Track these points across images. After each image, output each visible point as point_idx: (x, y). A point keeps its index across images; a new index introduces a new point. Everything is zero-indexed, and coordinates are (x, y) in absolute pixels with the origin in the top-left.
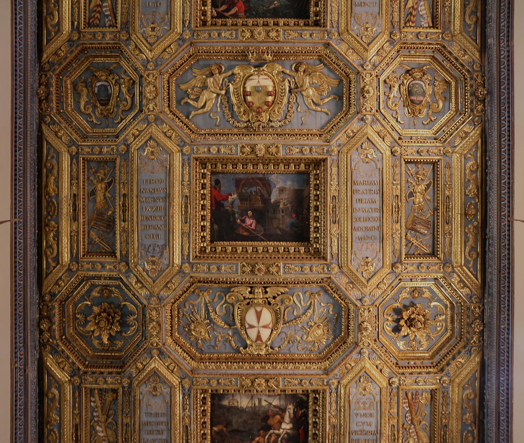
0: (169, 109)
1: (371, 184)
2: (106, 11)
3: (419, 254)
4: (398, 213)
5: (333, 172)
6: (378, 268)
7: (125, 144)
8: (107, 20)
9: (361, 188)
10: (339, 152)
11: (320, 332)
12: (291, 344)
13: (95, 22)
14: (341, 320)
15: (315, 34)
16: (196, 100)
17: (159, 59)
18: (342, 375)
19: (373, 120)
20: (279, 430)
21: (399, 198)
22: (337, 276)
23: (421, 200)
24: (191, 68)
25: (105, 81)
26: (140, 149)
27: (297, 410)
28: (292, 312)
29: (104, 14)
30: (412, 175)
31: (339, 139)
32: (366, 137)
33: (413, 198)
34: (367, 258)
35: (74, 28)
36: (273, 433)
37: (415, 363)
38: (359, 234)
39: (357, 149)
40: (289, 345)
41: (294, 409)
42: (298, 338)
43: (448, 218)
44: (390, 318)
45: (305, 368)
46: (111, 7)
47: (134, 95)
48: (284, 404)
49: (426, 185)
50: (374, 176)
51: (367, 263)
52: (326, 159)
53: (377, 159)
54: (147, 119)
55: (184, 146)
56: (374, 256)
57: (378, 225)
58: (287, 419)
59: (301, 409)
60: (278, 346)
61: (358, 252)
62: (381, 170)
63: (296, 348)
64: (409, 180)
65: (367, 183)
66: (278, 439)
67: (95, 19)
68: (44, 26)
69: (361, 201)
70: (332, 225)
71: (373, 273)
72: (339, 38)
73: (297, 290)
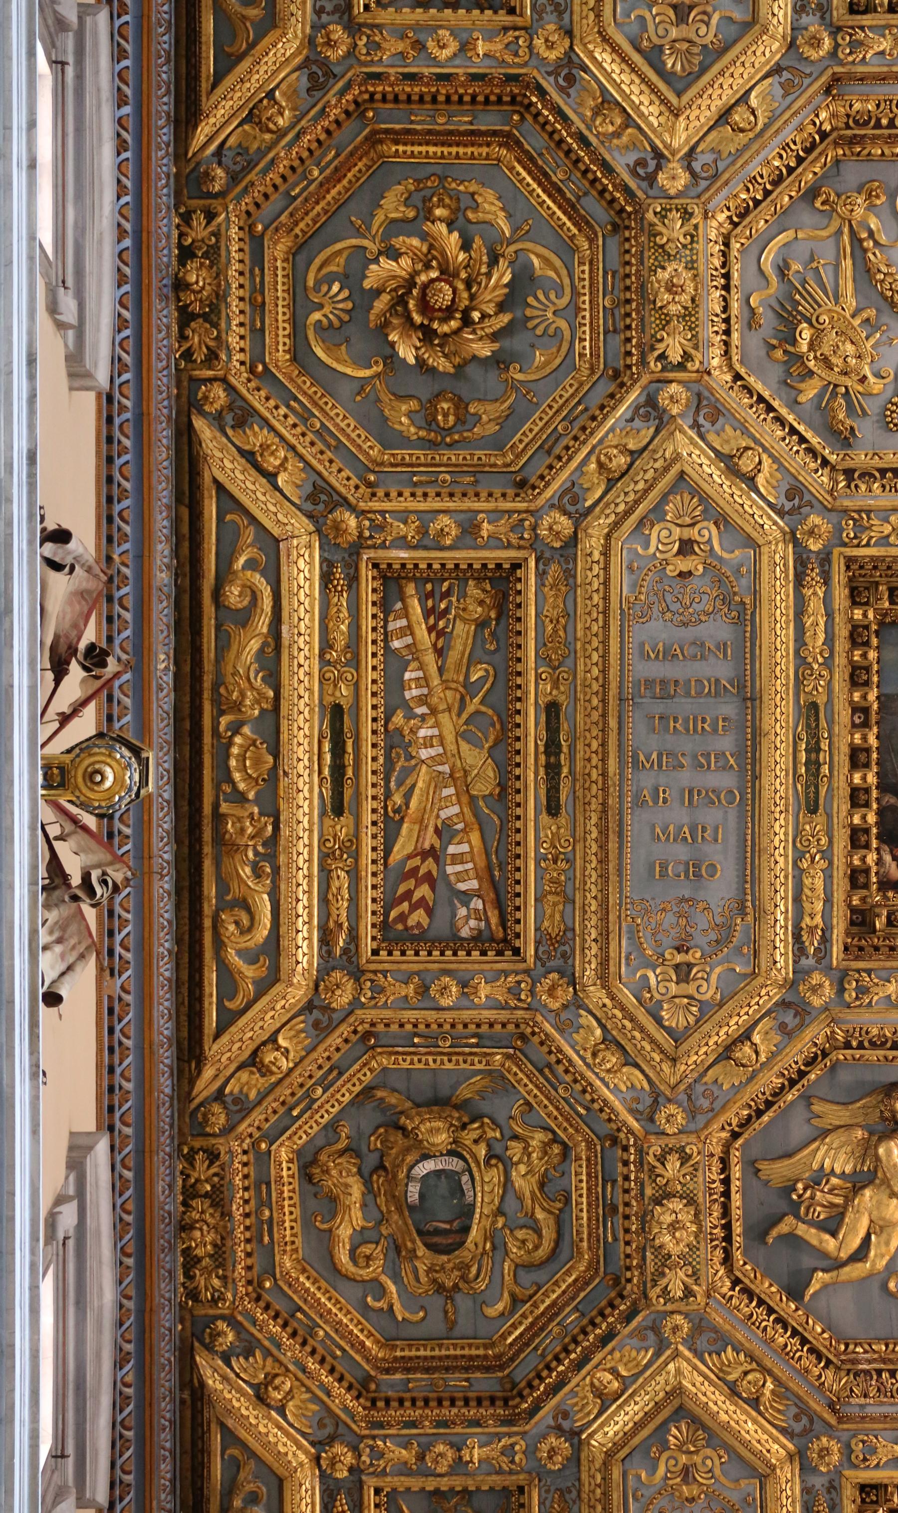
0: (730, 1271)
2: (461, 877)
7: (559, 1430)
8: (462, 912)
13: (411, 922)
16: (832, 1226)
17: (700, 1088)
24: (807, 1099)
25: (451, 1153)
26: (637, 1457)
29: (449, 884)
35: (329, 953)
46: (481, 863)
47: (567, 1200)
54: (656, 1329)
55: (806, 1432)
67: (413, 908)
68: (208, 954)
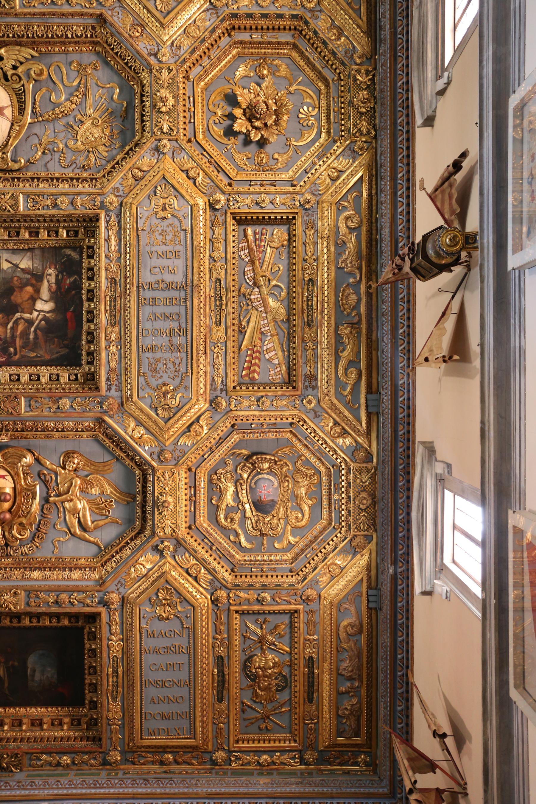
18: (127, 190)
20: (31, 313)
22: (115, 14)
27: (62, 278)
28: (48, 97)
36: (22, 318)
40: (45, 157)
41: (57, 276)
42: (61, 146)
48: (40, 267)
58: (45, 293)
59: (70, 275)
63: (57, 164)
66: (29, 328)
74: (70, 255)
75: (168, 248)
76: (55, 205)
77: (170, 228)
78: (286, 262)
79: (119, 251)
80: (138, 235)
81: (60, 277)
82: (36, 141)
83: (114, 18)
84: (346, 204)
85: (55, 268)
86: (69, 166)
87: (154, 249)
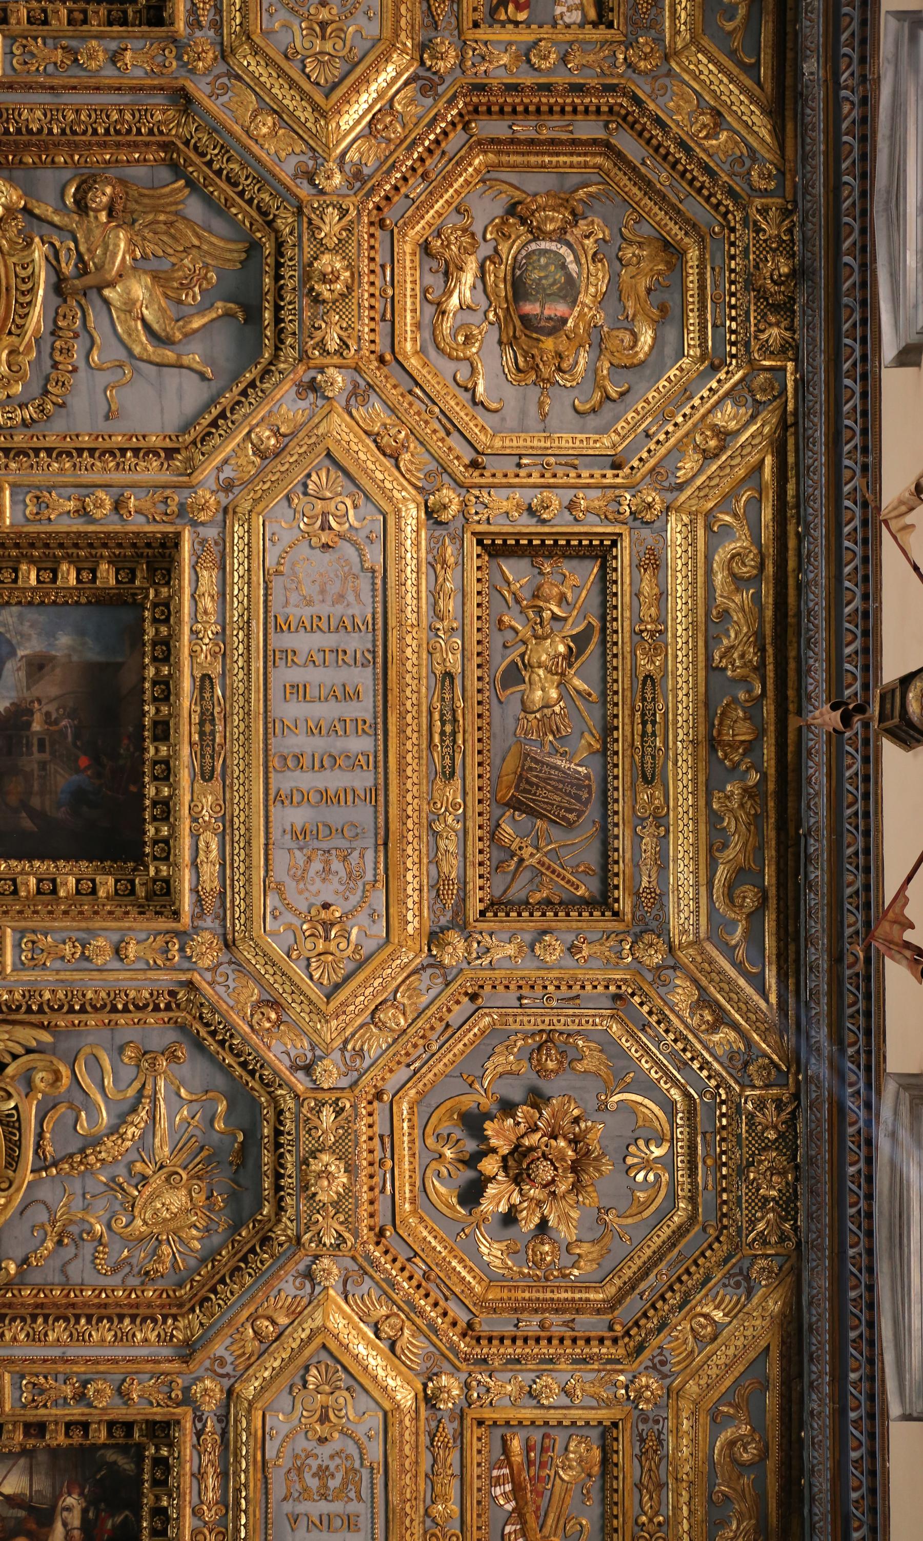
1: (341, 626)
3: (548, 902)
4: (454, 741)
5: (202, 589)
6: (369, 946)
9: (303, 642)
10: (225, 510)
11: (176, 1200)
12: (71, 1251)
14: (259, 1157)
15: (128, 54)
19: (356, 386)
21: (458, 682)
22: (220, 979)
23: (554, 694)
27: (97, 1516)
28: (71, 1122)
30: (517, 602)
31: (226, 462)
32: (320, 448)
33: (522, 687)
34: (326, 906)
37: (542, 1326)
38: (298, 816)
39: (288, 498)
40: (62, 1251)
41: (85, 1511)
43: (648, 759)
44: (449, 1154)
45: (109, 1337)
48: (48, 1492)
49: (574, 638)
50: (351, 598)
51: (328, 926)
52: (178, 535)
53: (363, 534)
56: (354, 899)
57: (370, 783)
60: (20, 1254)
61: (291, 886)
62: (379, 575)
63: (89, 1266)
64: (506, 619)
65: (324, 625)
69: (298, 690)
70: (199, 783)
71: (351, 966)
72: (221, 68)
73: (90, 1039)
74: (115, 1463)
75: (336, 1507)
76: (81, 1397)
77: (338, 1461)
78: (597, 1510)
79: (223, 1501)
80: (266, 1478)
81: (91, 1514)
82: (43, 1217)
83: (218, 988)
84: (728, 518)
85: (81, 1494)
86: (115, 1271)
87: (301, 1508)
